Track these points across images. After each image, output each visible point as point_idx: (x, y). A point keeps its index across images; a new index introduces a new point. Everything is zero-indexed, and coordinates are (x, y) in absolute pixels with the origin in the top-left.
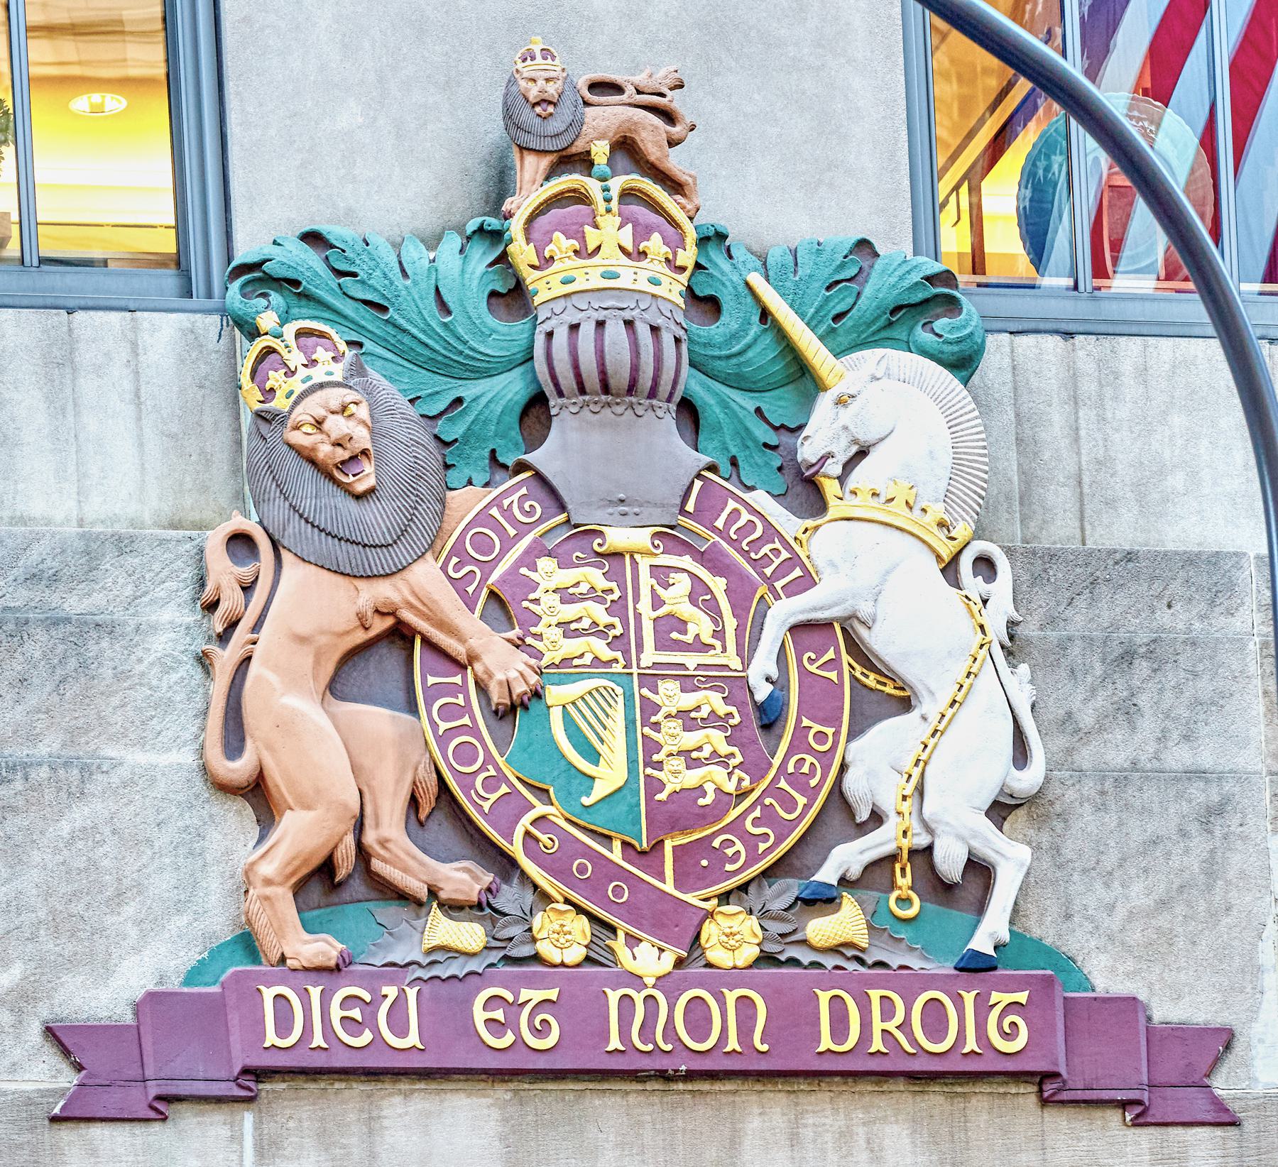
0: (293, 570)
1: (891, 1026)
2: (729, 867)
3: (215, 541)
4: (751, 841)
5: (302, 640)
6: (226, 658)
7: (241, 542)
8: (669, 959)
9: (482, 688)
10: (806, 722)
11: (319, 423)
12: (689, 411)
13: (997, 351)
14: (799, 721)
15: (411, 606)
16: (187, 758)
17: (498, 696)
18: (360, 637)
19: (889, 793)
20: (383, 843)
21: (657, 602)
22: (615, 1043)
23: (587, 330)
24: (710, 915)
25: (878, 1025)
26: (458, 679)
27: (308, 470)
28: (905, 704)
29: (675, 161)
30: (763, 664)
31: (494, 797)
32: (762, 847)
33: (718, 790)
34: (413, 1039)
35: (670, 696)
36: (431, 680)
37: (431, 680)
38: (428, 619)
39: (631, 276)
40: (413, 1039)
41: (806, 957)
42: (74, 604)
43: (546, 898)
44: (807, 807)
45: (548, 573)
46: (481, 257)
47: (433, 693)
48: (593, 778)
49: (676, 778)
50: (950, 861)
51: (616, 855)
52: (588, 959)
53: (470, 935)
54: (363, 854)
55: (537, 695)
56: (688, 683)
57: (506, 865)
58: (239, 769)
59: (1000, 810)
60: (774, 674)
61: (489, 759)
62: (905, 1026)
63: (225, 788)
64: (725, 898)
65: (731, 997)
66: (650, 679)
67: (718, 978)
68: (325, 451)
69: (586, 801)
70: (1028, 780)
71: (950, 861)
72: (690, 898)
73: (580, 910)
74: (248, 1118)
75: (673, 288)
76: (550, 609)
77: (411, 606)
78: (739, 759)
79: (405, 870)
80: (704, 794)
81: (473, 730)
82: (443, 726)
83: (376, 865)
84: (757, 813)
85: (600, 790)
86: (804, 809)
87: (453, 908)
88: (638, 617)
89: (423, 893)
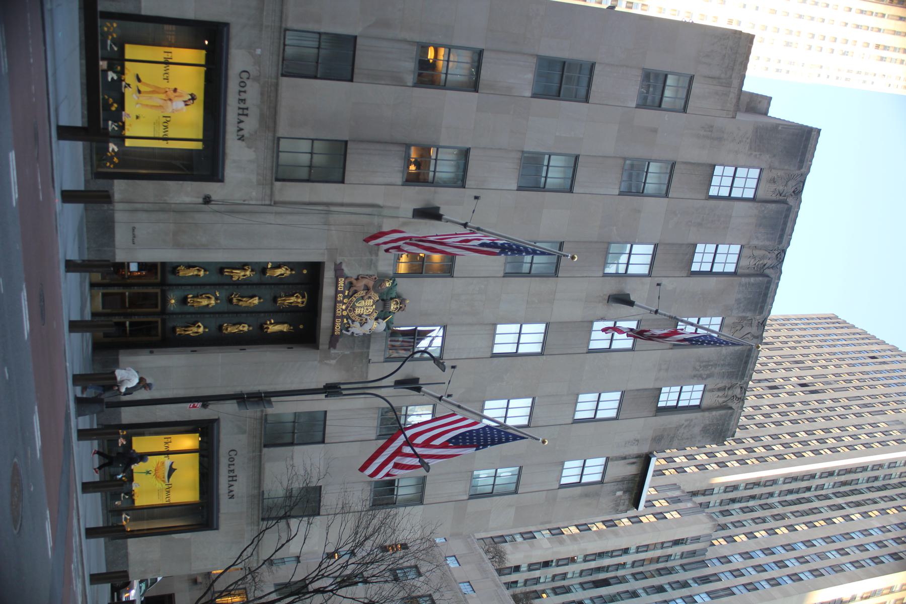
0: (373, 282)
3: (376, 276)
6: (367, 277)
7: (375, 278)
12: (382, 311)
13: (385, 333)
16: (361, 273)
19: (354, 325)
28: (361, 326)
29: (400, 311)
30: (364, 316)
35: (362, 309)
39: (392, 307)
42: (372, 266)
45: (372, 301)
46: (394, 296)
49: (357, 309)
50: (350, 329)
53: (346, 294)
57: (351, 296)
58: (360, 278)
59: (353, 333)
63: (358, 276)
67: (342, 312)
70: (355, 335)
71: (350, 329)
75: (391, 310)
76: (370, 300)
86: (353, 318)
87: (348, 293)
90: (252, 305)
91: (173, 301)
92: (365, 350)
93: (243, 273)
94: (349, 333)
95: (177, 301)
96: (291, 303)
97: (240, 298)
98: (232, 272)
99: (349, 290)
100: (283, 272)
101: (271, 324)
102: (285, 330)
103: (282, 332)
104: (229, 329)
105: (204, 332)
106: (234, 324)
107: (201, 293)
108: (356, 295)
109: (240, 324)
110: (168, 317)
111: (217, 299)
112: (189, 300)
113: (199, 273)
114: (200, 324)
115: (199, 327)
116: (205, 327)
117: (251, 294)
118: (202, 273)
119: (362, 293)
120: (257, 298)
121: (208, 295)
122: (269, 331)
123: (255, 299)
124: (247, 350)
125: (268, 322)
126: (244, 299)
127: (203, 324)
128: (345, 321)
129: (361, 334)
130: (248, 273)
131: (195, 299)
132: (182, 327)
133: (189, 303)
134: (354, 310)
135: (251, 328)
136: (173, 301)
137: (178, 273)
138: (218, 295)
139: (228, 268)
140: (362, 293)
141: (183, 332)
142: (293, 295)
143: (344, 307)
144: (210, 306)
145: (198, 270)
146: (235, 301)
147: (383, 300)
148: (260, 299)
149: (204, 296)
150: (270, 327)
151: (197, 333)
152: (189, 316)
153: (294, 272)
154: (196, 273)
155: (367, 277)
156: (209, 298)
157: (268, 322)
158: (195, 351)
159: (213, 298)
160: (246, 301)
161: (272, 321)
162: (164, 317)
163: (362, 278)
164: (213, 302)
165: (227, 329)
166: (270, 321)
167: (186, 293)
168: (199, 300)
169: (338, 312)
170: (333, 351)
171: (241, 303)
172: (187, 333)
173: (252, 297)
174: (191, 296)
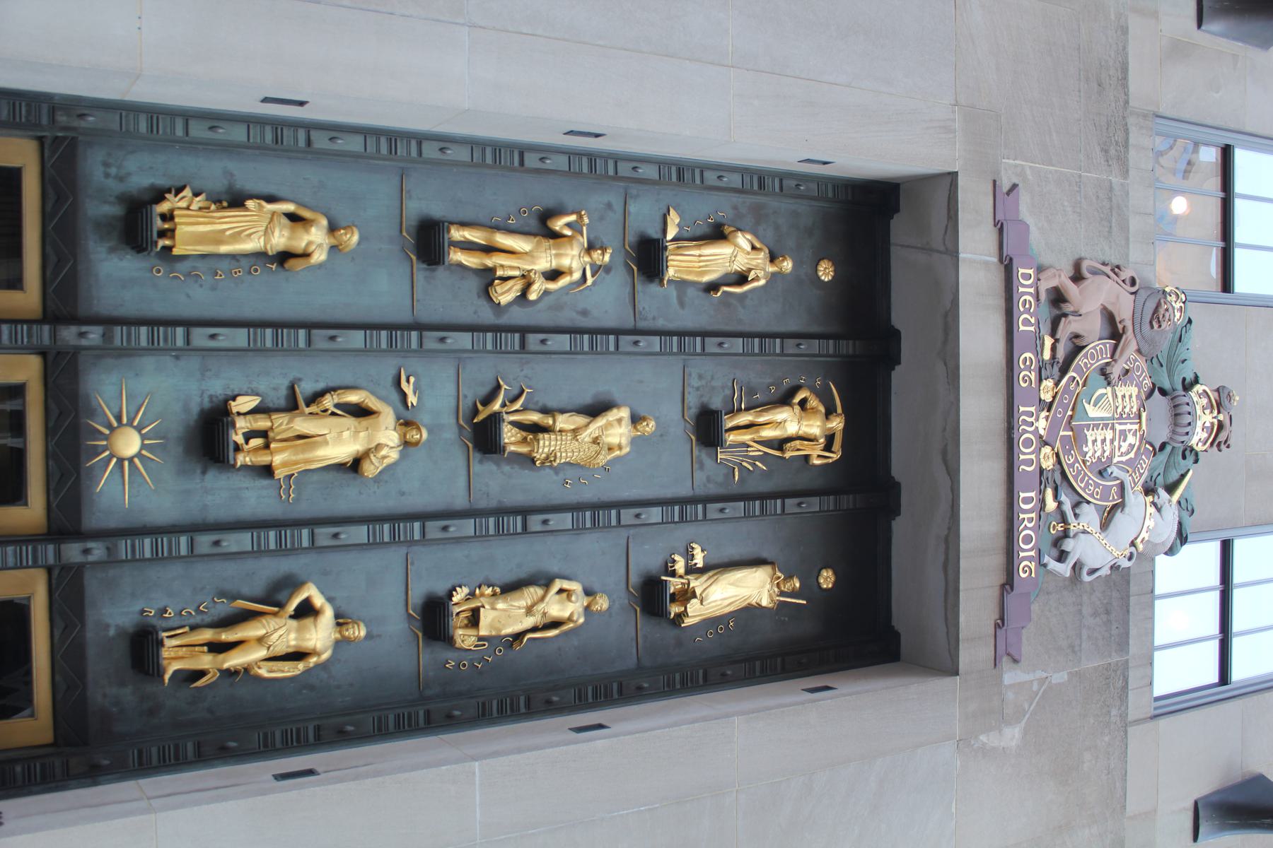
1: (1026, 522)
2: (1066, 456)
4: (1072, 466)
5: (1118, 297)
8: (1042, 432)
9: (1107, 364)
10: (1101, 487)
11: (1167, 310)
14: (1102, 485)
15: (1126, 339)
17: (1108, 370)
18: (1118, 320)
20: (1070, 322)
21: (1130, 431)
22: (1022, 409)
23: (1187, 408)
24: (1053, 450)
25: (1026, 516)
26: (1109, 356)
27: (1154, 306)
31: (1082, 365)
32: (1071, 470)
33: (1087, 453)
34: (1022, 328)
36: (1108, 345)
37: (1108, 345)
38: (1124, 345)
40: (1022, 328)
41: (1042, 487)
43: (1057, 384)
44: (1080, 487)
47: (1104, 344)
48: (1089, 404)
51: (1070, 413)
52: (1040, 400)
53: (1047, 355)
54: (1065, 315)
55: (1109, 384)
56: (1112, 441)
57: (1064, 370)
60: (1114, 475)
61: (1092, 365)
62: (1026, 528)
64: (1057, 455)
65: (1033, 457)
66: (1113, 428)
68: (1162, 311)
69: (1084, 401)
72: (1058, 443)
73: (1054, 397)
74: (995, 260)
77: (1126, 339)
78: (1094, 461)
79: (1063, 330)
80: (1086, 447)
81: (1098, 361)
82: (1098, 348)
83: (1063, 319)
84: (1080, 468)
85: (1087, 406)
87: (1054, 349)
88: (1126, 424)
89: (1058, 337)
90: (603, 459)
91: (129, 444)
92: (1116, 658)
93: (544, 262)
94: (1064, 569)
95: (155, 444)
96: (780, 444)
97: (535, 417)
98: (489, 249)
99: (1053, 334)
100: (740, 264)
101: (691, 570)
102: (765, 602)
103: (750, 612)
104: (486, 617)
105: (340, 644)
106: (510, 588)
107: (306, 388)
108: (1080, 360)
109: (544, 581)
110: (98, 550)
111: (406, 423)
112: (242, 424)
113: (300, 244)
114: (311, 592)
115: (306, 611)
116: (341, 620)
117: (587, 399)
118: (316, 238)
119: (1096, 351)
120: (624, 413)
121: (353, 398)
122: (695, 612)
123: (613, 415)
124: (615, 728)
125: (680, 567)
126: (564, 422)
127: (330, 600)
128: (1051, 505)
129: (1105, 571)
130: (572, 258)
131: (281, 423)
132: (193, 628)
133: (238, 448)
134: (1078, 439)
135: (602, 603)
136: (129, 444)
137: (168, 233)
138: (412, 399)
139: (463, 224)
140: (1096, 351)
141: (206, 661)
142: (784, 400)
143: (1042, 425)
144: (371, 469)
145: (293, 218)
146: (509, 436)
147: (1163, 392)
148: (635, 419)
149: (328, 402)
150: (697, 584)
151: (297, 655)
152: (242, 541)
153: (787, 265)
154: (280, 239)
155: (1107, 270)
156: (361, 412)
157: (680, 567)
158: (310, 772)
159: (387, 416)
160: (575, 432)
161: (699, 561)
162: (72, 552)
163: (1095, 272)
164: (387, 435)
165: (474, 619)
166: (689, 556)
167: (217, 388)
168: (301, 425)
169: (1025, 454)
170: (1011, 676)
171: (546, 445)
172: (234, 660)
173: (595, 410)
174: (244, 403)
